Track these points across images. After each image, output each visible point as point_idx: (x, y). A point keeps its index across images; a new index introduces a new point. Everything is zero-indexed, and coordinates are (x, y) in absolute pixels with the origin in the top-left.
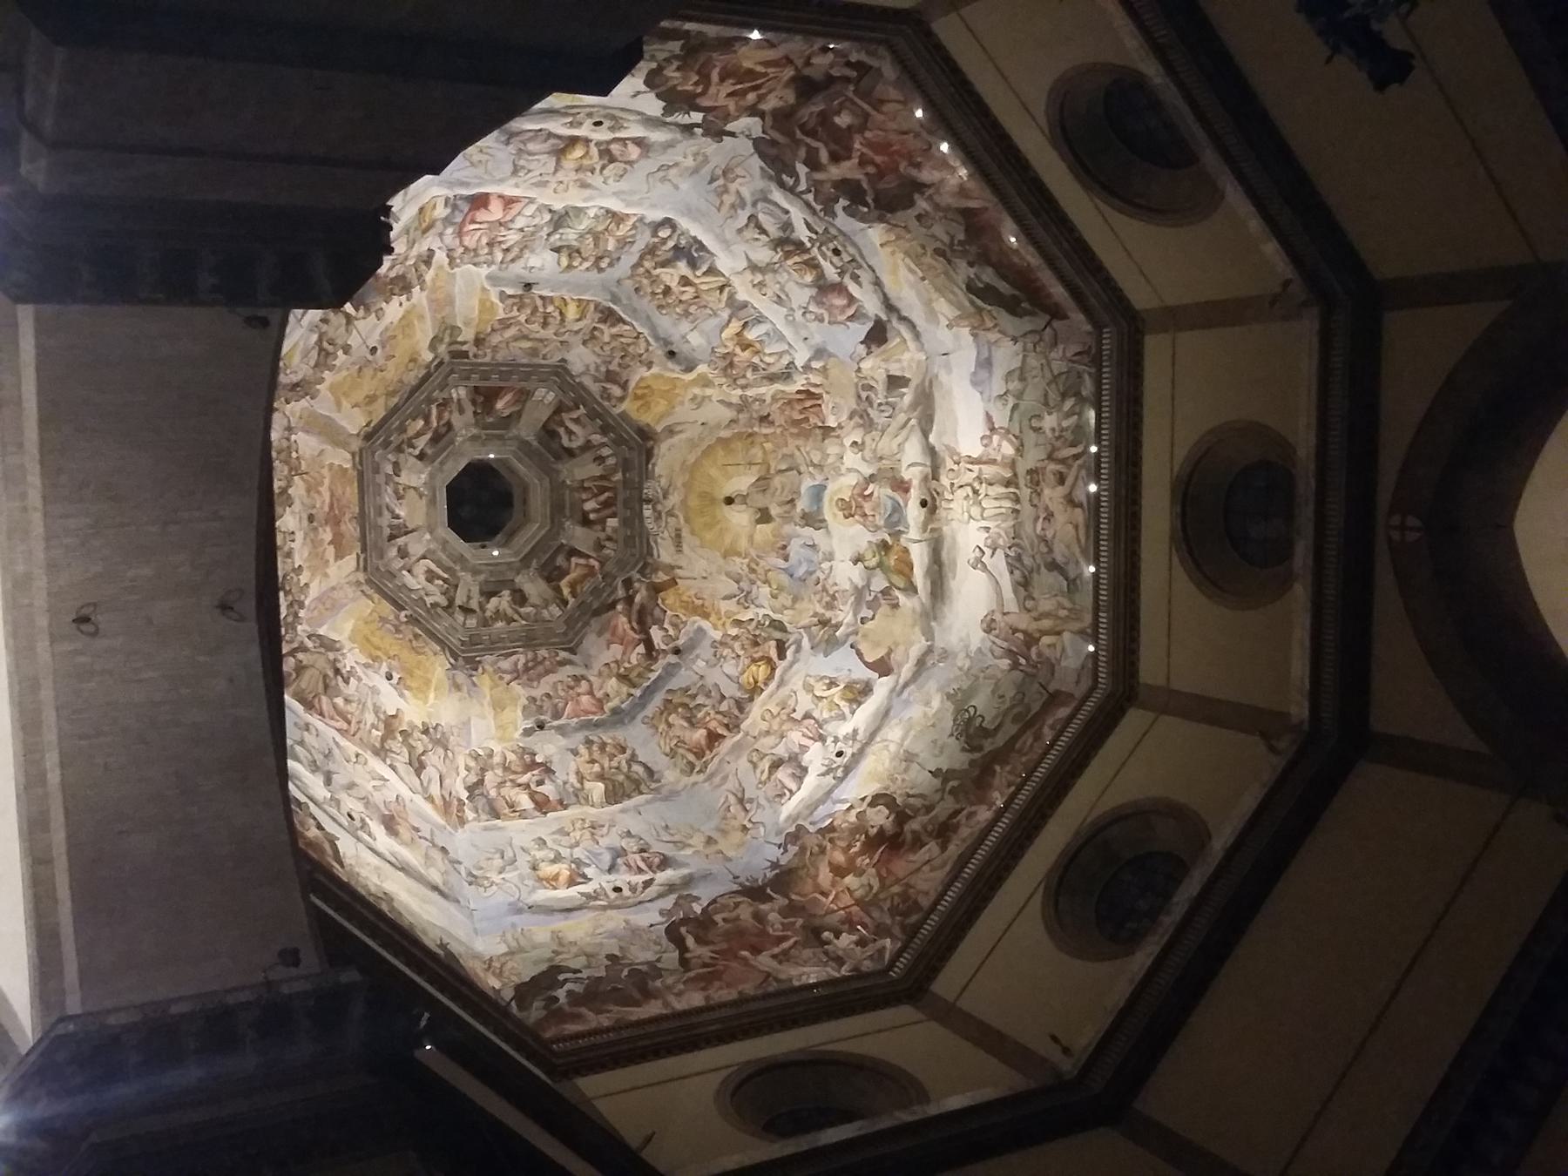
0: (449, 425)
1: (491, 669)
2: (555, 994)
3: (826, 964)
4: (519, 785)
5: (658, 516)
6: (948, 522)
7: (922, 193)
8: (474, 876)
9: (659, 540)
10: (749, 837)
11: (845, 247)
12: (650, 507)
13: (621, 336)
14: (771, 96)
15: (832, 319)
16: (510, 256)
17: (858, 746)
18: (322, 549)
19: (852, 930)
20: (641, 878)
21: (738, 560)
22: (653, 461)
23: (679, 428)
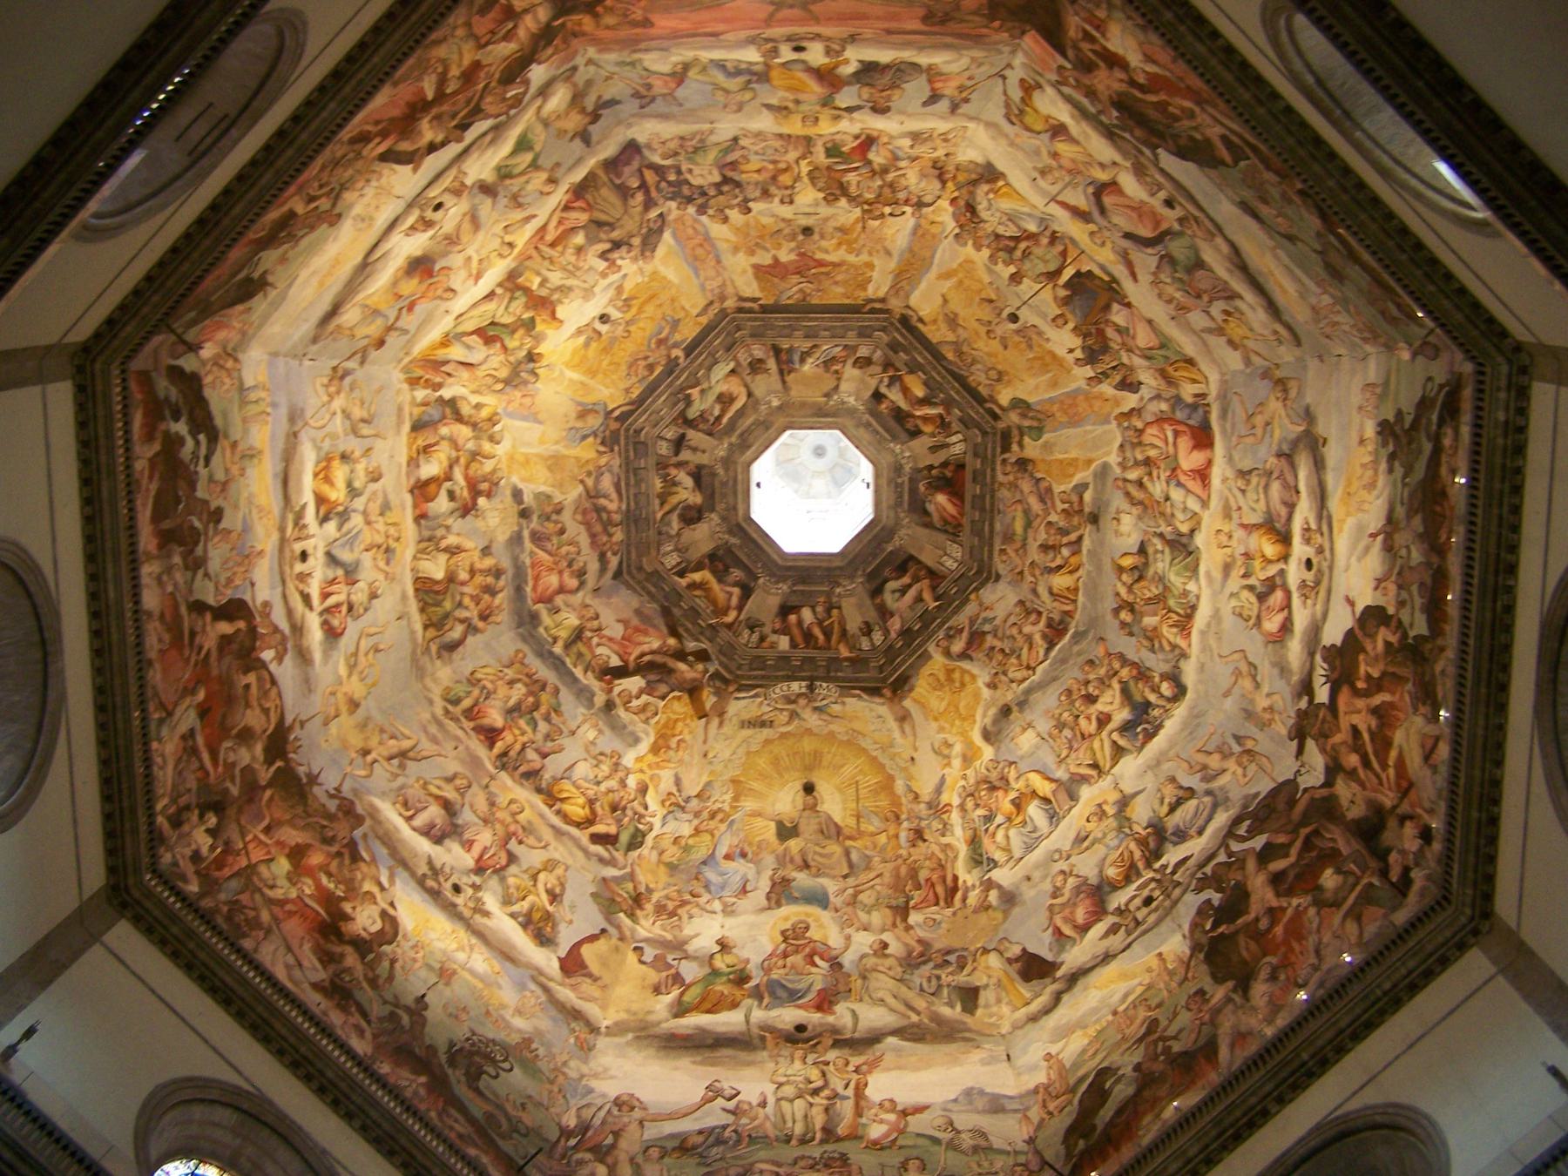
0: (916, 433)
1: (603, 460)
2: (183, 419)
3: (174, 800)
4: (451, 467)
6: (775, 1058)
7: (1234, 990)
8: (342, 378)
10: (354, 755)
11: (1156, 909)
14: (1355, 786)
15: (1057, 909)
17: (467, 913)
19: (212, 848)
20: (314, 590)
21: (728, 797)
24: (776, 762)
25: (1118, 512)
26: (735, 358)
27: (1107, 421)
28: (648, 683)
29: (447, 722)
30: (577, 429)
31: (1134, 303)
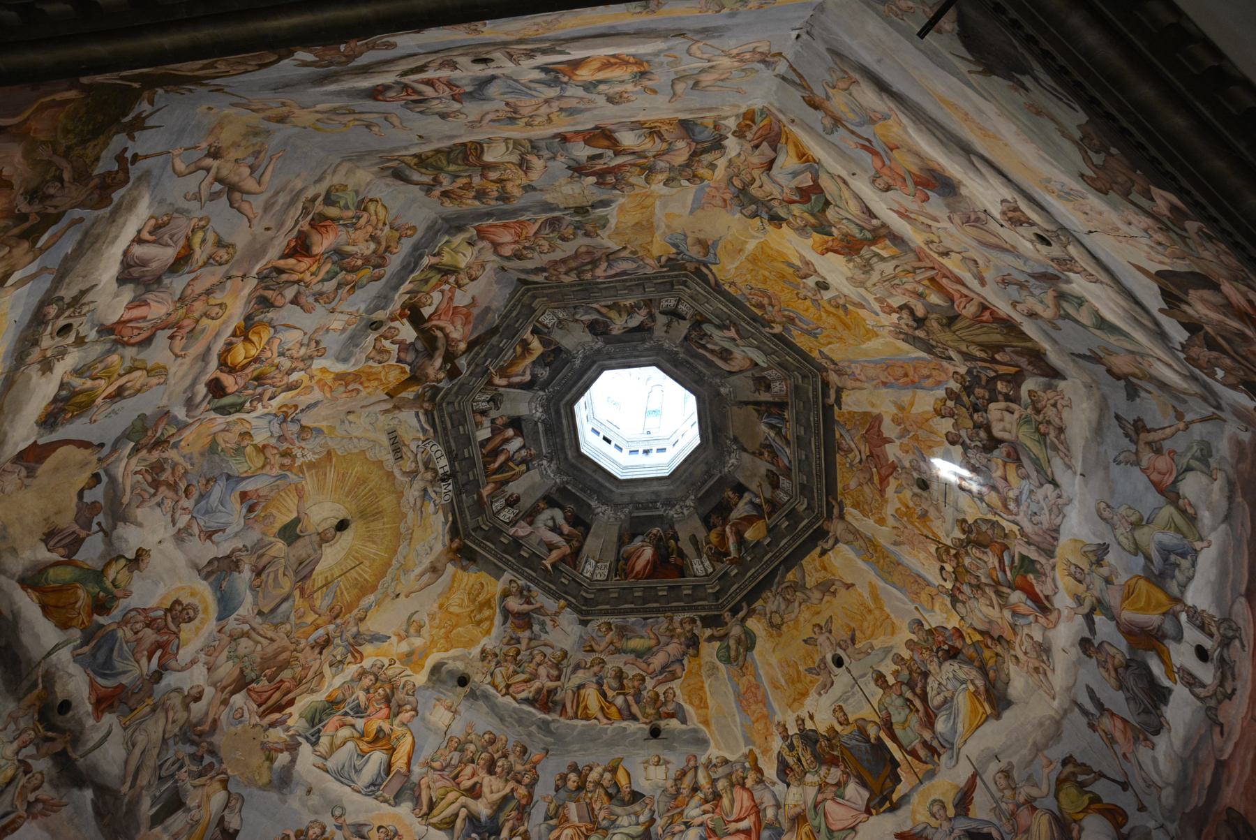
0: (709, 527)
1: (648, 261)
4: (633, 153)
8: (763, 61)
9: (421, 435)
10: (204, 145)
12: (441, 471)
16: (687, 782)
18: (905, 440)
20: (429, 74)
21: (311, 457)
24: (362, 481)
26: (769, 368)
27: (748, 741)
28: (412, 344)
29: (300, 206)
31: (872, 819)
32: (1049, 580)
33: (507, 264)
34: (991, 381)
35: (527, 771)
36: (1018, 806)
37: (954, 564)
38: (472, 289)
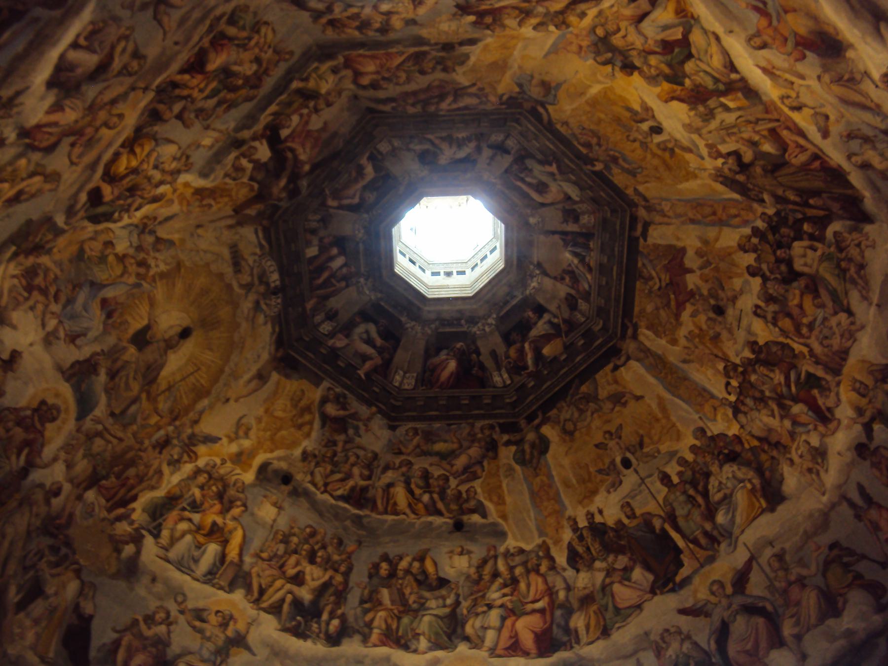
1: (493, 99)
5: (263, 278)
9: (258, 251)
12: (273, 285)
13: (342, 480)
16: (488, 569)
18: (706, 271)
21: (163, 267)
22: (274, 337)
23: (253, 385)
25: (469, 552)
26: (581, 202)
27: (541, 533)
28: (265, 164)
29: (208, 23)
30: (530, 81)
31: (656, 598)
32: (833, 394)
33: (361, 93)
34: (799, 223)
35: (343, 561)
36: (790, 584)
37: (740, 379)
38: (327, 113)
